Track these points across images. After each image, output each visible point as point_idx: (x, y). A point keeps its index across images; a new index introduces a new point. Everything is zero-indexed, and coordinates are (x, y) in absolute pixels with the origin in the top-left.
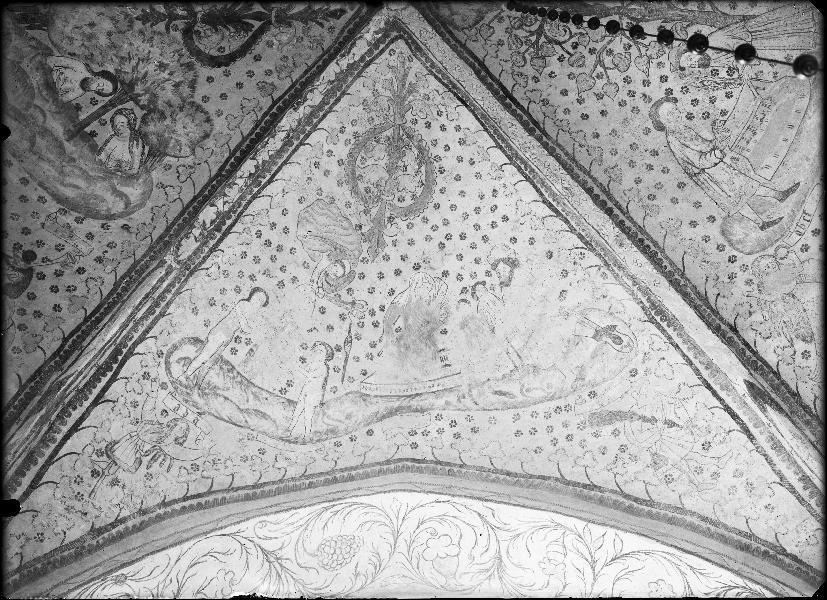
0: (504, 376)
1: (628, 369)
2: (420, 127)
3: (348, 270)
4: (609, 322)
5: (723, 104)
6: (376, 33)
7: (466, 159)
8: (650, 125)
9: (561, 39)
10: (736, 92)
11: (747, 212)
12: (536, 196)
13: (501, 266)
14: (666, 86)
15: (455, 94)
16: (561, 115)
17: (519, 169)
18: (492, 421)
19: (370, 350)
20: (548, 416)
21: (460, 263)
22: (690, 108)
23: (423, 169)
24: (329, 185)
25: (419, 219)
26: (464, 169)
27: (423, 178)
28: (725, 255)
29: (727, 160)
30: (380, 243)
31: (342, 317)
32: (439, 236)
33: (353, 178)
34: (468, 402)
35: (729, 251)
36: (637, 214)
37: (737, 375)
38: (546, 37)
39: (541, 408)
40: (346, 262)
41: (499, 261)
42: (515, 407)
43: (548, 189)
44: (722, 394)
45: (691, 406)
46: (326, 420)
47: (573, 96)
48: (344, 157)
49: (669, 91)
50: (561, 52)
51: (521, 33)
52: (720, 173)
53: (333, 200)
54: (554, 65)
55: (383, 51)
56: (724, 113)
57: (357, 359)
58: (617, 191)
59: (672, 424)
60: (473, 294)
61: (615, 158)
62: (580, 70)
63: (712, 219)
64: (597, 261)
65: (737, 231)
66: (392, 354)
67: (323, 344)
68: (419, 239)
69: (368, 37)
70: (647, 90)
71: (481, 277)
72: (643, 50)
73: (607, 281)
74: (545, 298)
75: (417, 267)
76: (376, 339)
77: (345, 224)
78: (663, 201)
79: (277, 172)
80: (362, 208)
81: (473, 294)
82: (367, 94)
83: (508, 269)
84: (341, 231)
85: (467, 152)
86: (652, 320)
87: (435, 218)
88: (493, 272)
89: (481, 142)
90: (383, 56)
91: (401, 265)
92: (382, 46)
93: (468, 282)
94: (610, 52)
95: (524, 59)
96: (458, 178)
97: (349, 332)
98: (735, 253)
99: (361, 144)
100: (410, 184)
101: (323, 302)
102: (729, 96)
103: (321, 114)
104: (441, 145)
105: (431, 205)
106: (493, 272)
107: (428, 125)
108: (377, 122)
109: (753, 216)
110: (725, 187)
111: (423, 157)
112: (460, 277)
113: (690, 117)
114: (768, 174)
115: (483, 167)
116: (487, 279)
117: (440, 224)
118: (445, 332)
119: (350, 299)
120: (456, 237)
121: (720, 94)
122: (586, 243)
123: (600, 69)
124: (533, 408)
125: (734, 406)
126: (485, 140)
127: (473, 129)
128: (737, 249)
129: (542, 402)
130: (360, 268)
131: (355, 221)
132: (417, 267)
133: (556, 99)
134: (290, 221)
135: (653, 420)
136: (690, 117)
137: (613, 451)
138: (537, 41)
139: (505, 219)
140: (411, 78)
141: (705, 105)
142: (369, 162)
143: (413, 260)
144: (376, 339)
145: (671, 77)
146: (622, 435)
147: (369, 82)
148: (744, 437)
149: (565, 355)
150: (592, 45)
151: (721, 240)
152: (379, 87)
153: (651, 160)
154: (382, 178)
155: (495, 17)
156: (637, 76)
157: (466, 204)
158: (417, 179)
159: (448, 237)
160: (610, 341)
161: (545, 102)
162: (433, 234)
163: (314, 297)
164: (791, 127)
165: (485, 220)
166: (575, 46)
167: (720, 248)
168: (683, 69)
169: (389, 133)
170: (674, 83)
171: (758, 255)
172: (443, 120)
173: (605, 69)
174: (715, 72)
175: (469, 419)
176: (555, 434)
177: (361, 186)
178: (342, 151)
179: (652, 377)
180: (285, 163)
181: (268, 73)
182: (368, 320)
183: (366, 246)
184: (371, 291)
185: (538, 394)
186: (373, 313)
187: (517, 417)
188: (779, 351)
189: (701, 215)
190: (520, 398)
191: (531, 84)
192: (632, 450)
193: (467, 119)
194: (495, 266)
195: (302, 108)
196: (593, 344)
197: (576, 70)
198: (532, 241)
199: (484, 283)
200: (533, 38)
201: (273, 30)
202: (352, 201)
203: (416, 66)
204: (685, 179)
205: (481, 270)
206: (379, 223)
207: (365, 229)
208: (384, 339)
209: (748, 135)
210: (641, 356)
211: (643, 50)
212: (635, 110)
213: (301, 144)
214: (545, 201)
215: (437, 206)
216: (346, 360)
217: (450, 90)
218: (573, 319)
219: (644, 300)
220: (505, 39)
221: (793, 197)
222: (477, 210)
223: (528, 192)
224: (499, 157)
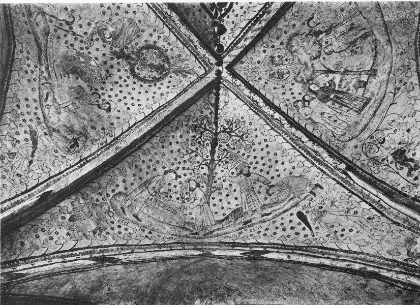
0: (55, 99)
1: (58, 149)
2: (168, 79)
3: (107, 40)
5: (174, 196)
6: (208, 59)
7: (154, 95)
8: (167, 169)
9: (202, 138)
10: (179, 201)
11: (129, 203)
12: (138, 120)
13: (108, 106)
14: (182, 176)
15: (182, 92)
16: (172, 134)
17: (149, 115)
18: (33, 90)
19: (70, 43)
20: (35, 114)
21: (109, 89)
22: (173, 184)
23: (151, 79)
24: (145, 36)
25: (129, 74)
26: (150, 95)
27: (147, 79)
28: (109, 193)
29: (151, 197)
30: (118, 58)
31: (86, 33)
32: (121, 82)
33: (148, 47)
34: (43, 81)
35: (112, 195)
36: (129, 159)
37: (54, 188)
38: (203, 132)
39: (39, 112)
40: (111, 40)
41: (109, 104)
42: (40, 101)
43: (141, 124)
44: (45, 184)
45: (40, 171)
46: (36, 13)
47: (179, 140)
48: (157, 44)
49: (180, 177)
50: (197, 137)
51: (205, 121)
52: (145, 194)
53: (139, 36)
54: (192, 134)
55: (201, 64)
56: (171, 197)
57: (65, 36)
58: (139, 153)
59: (31, 162)
60: (94, 93)
61: (153, 153)
62: (190, 144)
63: (126, 189)
64: (109, 141)
65: (121, 198)
66: (67, 53)
67: (73, 21)
68: (120, 74)
69: (207, 55)
70: (181, 169)
71: (102, 97)
72: (197, 168)
73: (100, 145)
74: (92, 120)
75: (108, 71)
76: (75, 47)
77: (128, 41)
78: (134, 170)
79: (152, 10)
80: (135, 50)
81: (94, 93)
82: (184, 56)
83: (106, 108)
84: (125, 39)
85: (158, 96)
86: (81, 160)
87: (129, 82)
88: (104, 102)
89: (162, 100)
90: (198, 63)
91: (108, 65)
92: (203, 63)
93: (100, 92)
94: (196, 156)
95: (195, 122)
96: (147, 92)
97: (78, 35)
98: (111, 196)
99: (162, 53)
100: (144, 73)
101: (93, 25)
102: (178, 199)
103: (176, 34)
104: (161, 86)
105: (135, 80)
106: (104, 102)
107: (169, 82)
108: (172, 61)
109: (127, 205)
110: (140, 195)
111: (155, 80)
112: (102, 89)
113: (169, 184)
114: (145, 211)
115: (151, 101)
116: (101, 99)
117: (127, 83)
118: (77, 79)
119: (94, 38)
120: (121, 89)
121: (178, 196)
122: (117, 138)
123: (190, 151)
124: (39, 107)
125: (39, 187)
126: (162, 102)
127: (167, 98)
128: (112, 198)
129: (43, 112)
130: (108, 46)
131: (129, 46)
132: (108, 71)
133: (178, 134)
134: (131, 15)
135: (33, 156)
136: (169, 184)
137: (17, 138)
138: (201, 127)
139: (128, 109)
140: (189, 76)
141: (175, 190)
142: (154, 56)
143: (111, 70)
144: (75, 47)
146: (25, 142)
147: (188, 58)
148: (23, 190)
149: (65, 126)
150: (199, 149)
151: (117, 191)
152: (186, 62)
153: (152, 168)
154: (147, 61)
155: (212, 111)
156: (186, 166)
157: (135, 94)
158: (147, 76)
159: (121, 86)
160: (72, 144)
161: (177, 128)
162: (122, 80)
163: (96, 21)
164: (164, 220)
165: (128, 100)
166: (199, 143)
167: (113, 191)
168: (189, 182)
169: (166, 66)
170: (183, 179)
171: (110, 205)
172: (171, 87)
173: (190, 153)
174: (187, 193)
175: (35, 80)
176: (26, 115)
177: (144, 51)
178: (160, 44)
179: (53, 158)
180: (156, 14)
181: (194, 14)
182: (84, 46)
183: (118, 50)
184: (97, 50)
185: (46, 111)
186: (87, 48)
187: (35, 101)
188: (65, 208)
189: (128, 185)
190: (45, 104)
191: (185, 123)
192: (18, 146)
193: (171, 96)
194: (107, 103)
195: (179, 22)
196: (70, 137)
197: (189, 142)
198: (118, 118)
199: (100, 98)
200: (203, 126)
201: (211, 20)
202: (138, 46)
203: (194, 78)
204: (144, 180)
205: (106, 97)
206: (128, 57)
207: (125, 50)
208: (74, 51)
209: (162, 205)
210: (65, 155)
211: (197, 168)
212: (173, 164)
213: (164, 24)
215: (134, 83)
216: (66, 31)
217: (184, 90)
218: (82, 131)
219: (90, 158)
220: (203, 114)
221: (135, 220)
222: (132, 98)
223: (140, 117)
224: (155, 107)
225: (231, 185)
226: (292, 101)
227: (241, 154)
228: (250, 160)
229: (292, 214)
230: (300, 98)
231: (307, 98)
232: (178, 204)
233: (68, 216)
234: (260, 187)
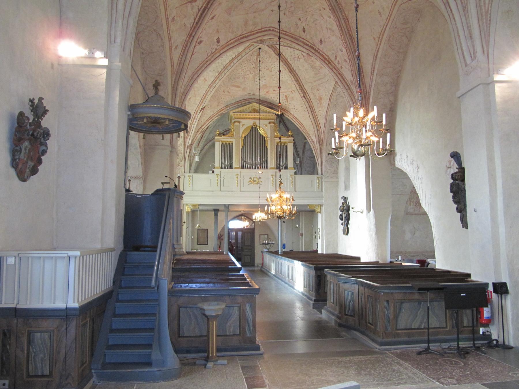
4: (207, 79)
5: (241, 77)
49: (243, 70)
102: (242, 78)
113: (239, 73)
121: (243, 77)
136: (239, 73)
145: (246, 70)
170: (245, 70)
214: (226, 65)
224: (234, 56)
225: (263, 73)
226: (293, 56)
227: (269, 62)
228: (273, 66)
229: (283, 95)
230: (297, 56)
231: (299, 57)
232: (243, 80)
233: (209, 106)
234: (275, 78)
